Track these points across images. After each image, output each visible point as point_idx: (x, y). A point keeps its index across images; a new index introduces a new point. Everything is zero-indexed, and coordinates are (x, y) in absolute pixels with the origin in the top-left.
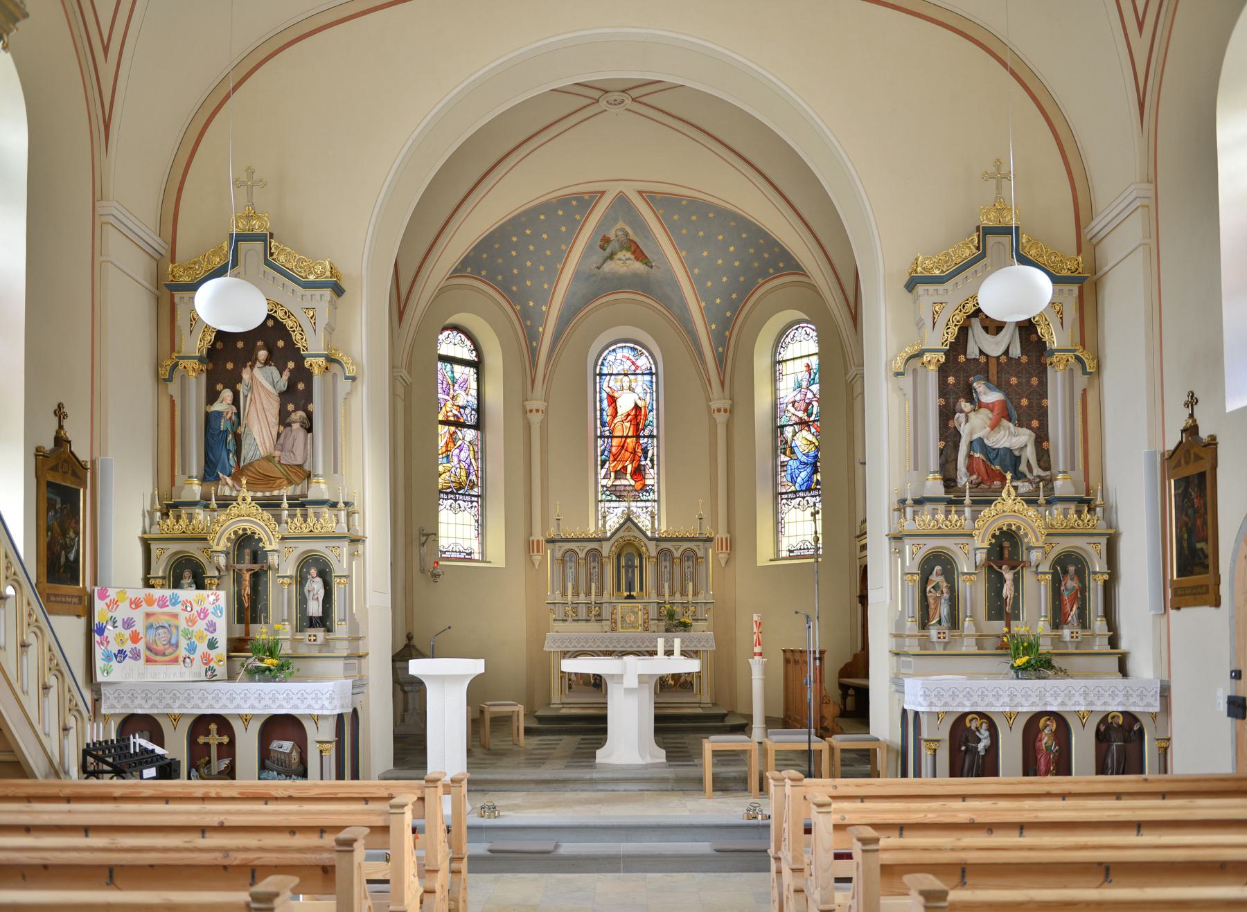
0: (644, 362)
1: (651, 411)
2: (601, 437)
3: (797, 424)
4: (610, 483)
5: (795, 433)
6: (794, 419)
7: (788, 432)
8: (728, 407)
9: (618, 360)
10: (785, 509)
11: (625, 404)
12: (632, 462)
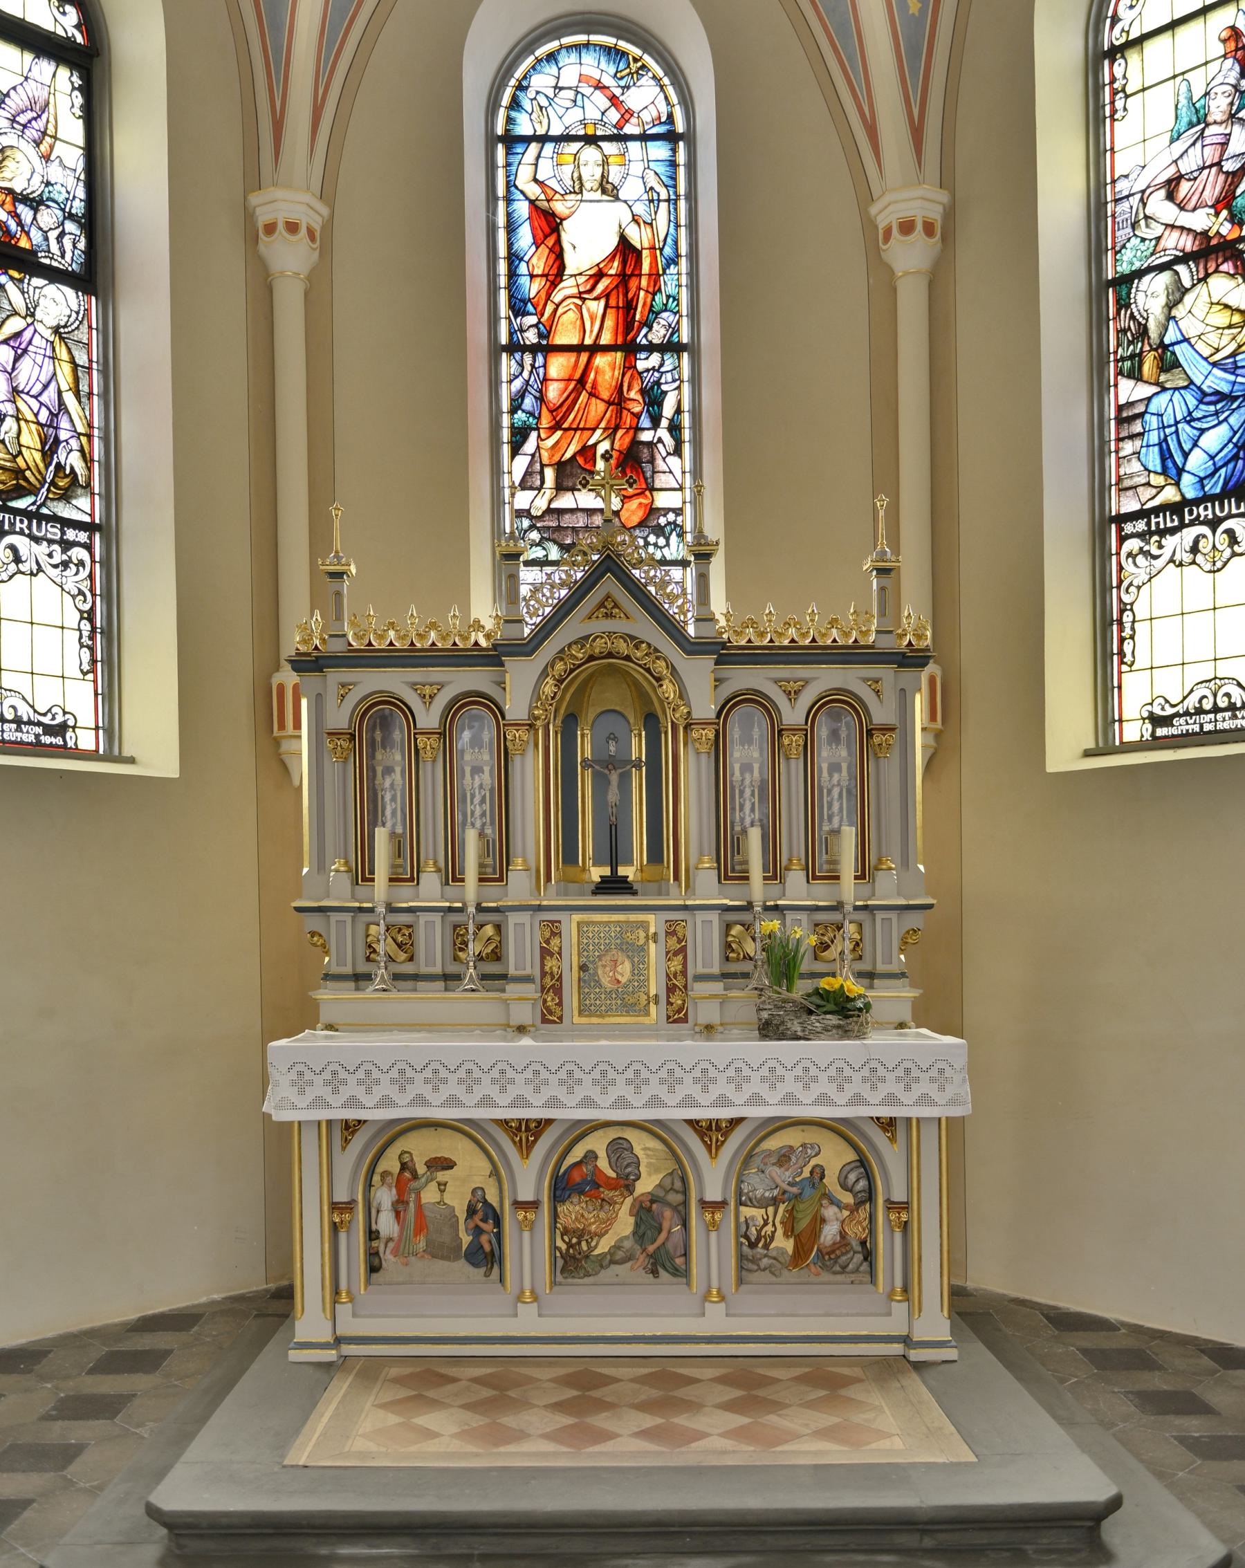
0: (647, 99)
1: (674, 261)
2: (514, 348)
3: (1184, 258)
4: (541, 504)
5: (1178, 294)
6: (1175, 243)
7: (1150, 296)
8: (935, 214)
9: (569, 87)
10: (1136, 571)
11: (589, 238)
12: (611, 432)
